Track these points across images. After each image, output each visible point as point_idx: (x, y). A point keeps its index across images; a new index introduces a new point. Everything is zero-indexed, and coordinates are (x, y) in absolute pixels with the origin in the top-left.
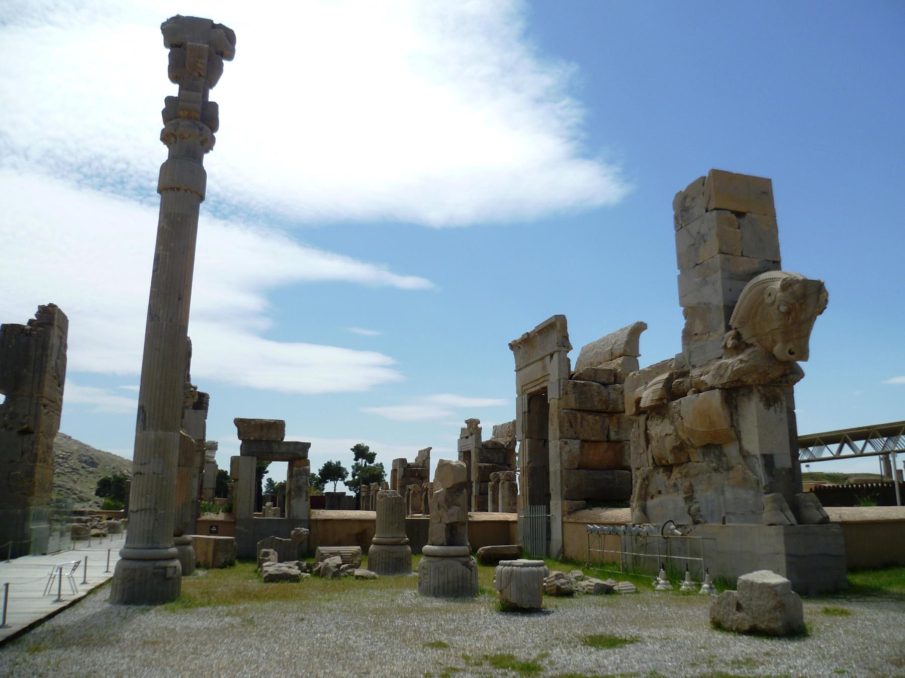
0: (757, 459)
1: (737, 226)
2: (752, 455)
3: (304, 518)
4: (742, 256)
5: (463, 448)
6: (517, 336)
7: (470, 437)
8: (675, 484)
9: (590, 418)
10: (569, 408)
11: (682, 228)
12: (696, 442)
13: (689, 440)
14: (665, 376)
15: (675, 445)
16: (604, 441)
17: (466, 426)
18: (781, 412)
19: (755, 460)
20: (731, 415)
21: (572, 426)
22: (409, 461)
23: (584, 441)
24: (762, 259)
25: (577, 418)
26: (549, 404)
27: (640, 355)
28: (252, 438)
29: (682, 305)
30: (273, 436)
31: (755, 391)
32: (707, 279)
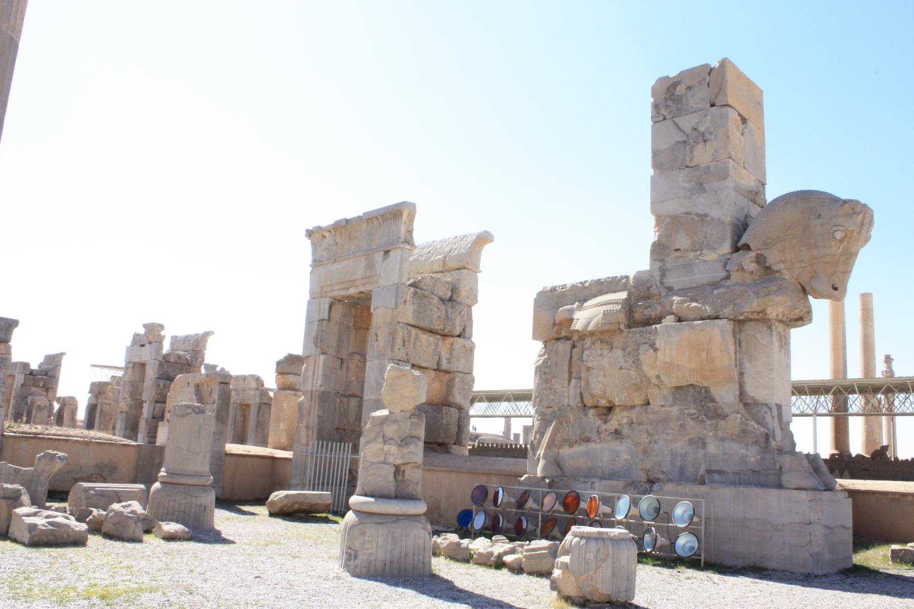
0: (770, 408)
2: (762, 404)
4: (744, 168)
6: (327, 221)
8: (616, 430)
9: (425, 337)
10: (406, 321)
11: (665, 119)
12: (671, 381)
13: (658, 377)
14: (623, 295)
16: (431, 369)
17: (142, 331)
19: (765, 409)
21: (404, 346)
25: (410, 336)
26: (372, 314)
27: (480, 271)
29: (653, 211)
31: (773, 327)
32: (704, 185)
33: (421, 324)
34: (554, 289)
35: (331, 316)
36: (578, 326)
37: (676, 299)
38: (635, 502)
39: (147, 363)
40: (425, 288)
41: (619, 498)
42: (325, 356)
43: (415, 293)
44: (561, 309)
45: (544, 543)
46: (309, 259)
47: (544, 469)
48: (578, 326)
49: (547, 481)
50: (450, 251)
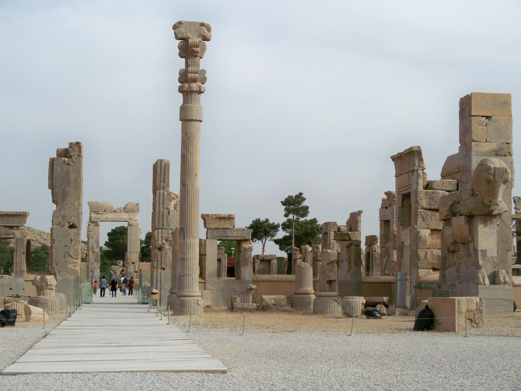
1: (485, 124)
3: (250, 280)
5: (383, 217)
7: (389, 208)
15: (452, 241)
18: (493, 229)
20: (470, 229)
22: (339, 224)
23: (432, 230)
24: (499, 143)
28: (213, 227)
30: (227, 226)
33: (432, 208)
35: (404, 205)
39: (390, 220)
40: (436, 188)
42: (402, 226)
43: (427, 193)
46: (394, 173)
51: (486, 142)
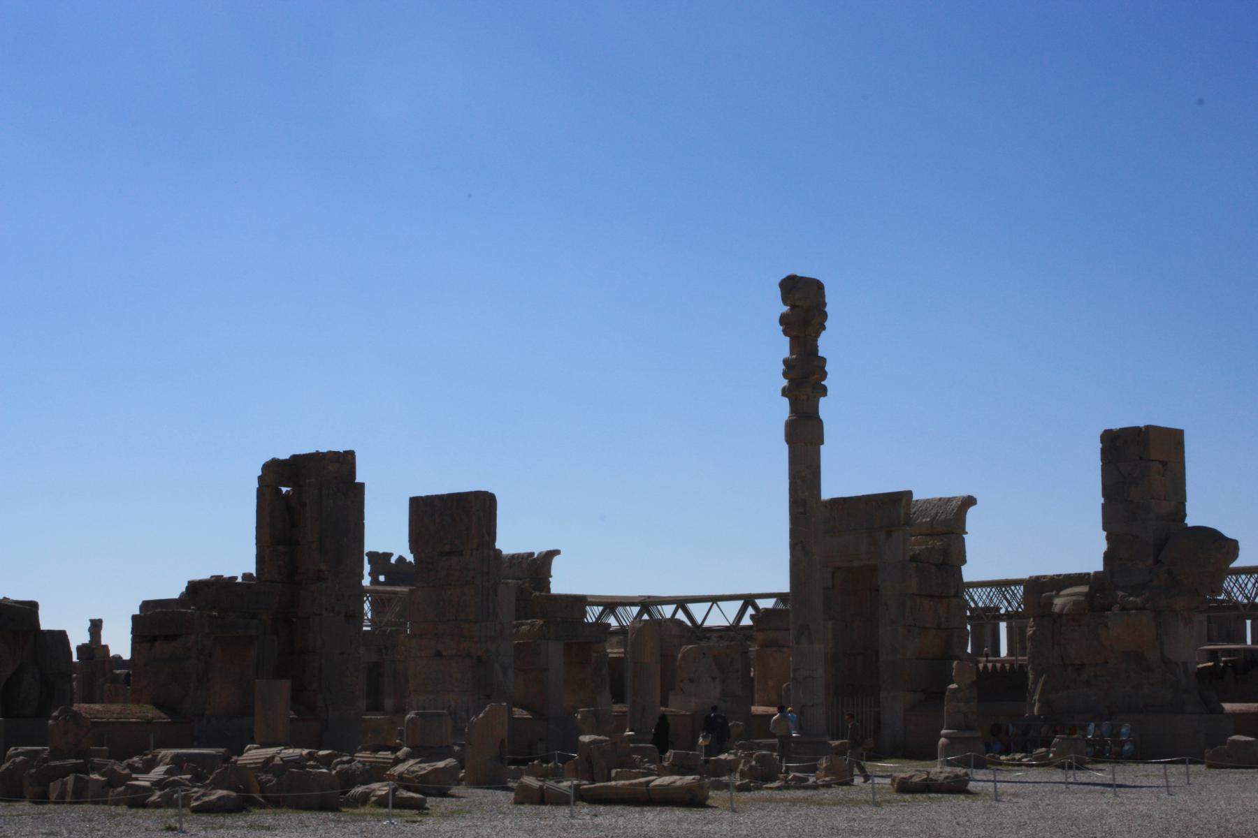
14: (1085, 589)
27: (966, 533)
34: (1038, 578)
36: (1056, 609)
37: (1120, 593)
38: (1098, 727)
41: (1089, 725)
44: (1044, 595)
45: (1044, 749)
47: (1040, 709)
48: (1056, 609)
49: (1042, 717)
50: (937, 515)
51: (1165, 500)
